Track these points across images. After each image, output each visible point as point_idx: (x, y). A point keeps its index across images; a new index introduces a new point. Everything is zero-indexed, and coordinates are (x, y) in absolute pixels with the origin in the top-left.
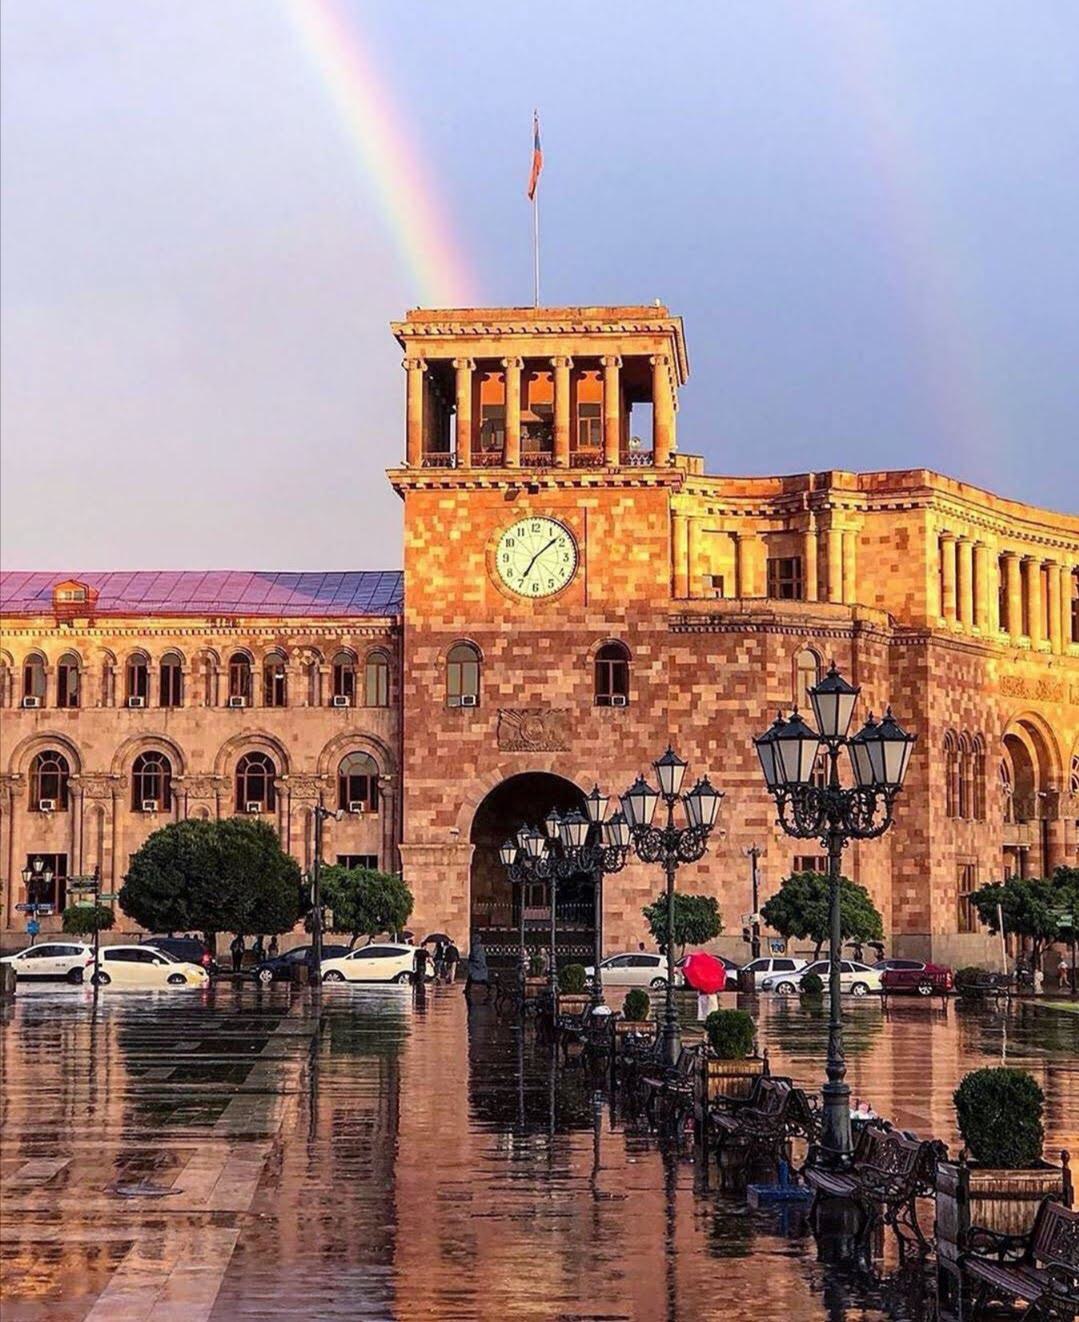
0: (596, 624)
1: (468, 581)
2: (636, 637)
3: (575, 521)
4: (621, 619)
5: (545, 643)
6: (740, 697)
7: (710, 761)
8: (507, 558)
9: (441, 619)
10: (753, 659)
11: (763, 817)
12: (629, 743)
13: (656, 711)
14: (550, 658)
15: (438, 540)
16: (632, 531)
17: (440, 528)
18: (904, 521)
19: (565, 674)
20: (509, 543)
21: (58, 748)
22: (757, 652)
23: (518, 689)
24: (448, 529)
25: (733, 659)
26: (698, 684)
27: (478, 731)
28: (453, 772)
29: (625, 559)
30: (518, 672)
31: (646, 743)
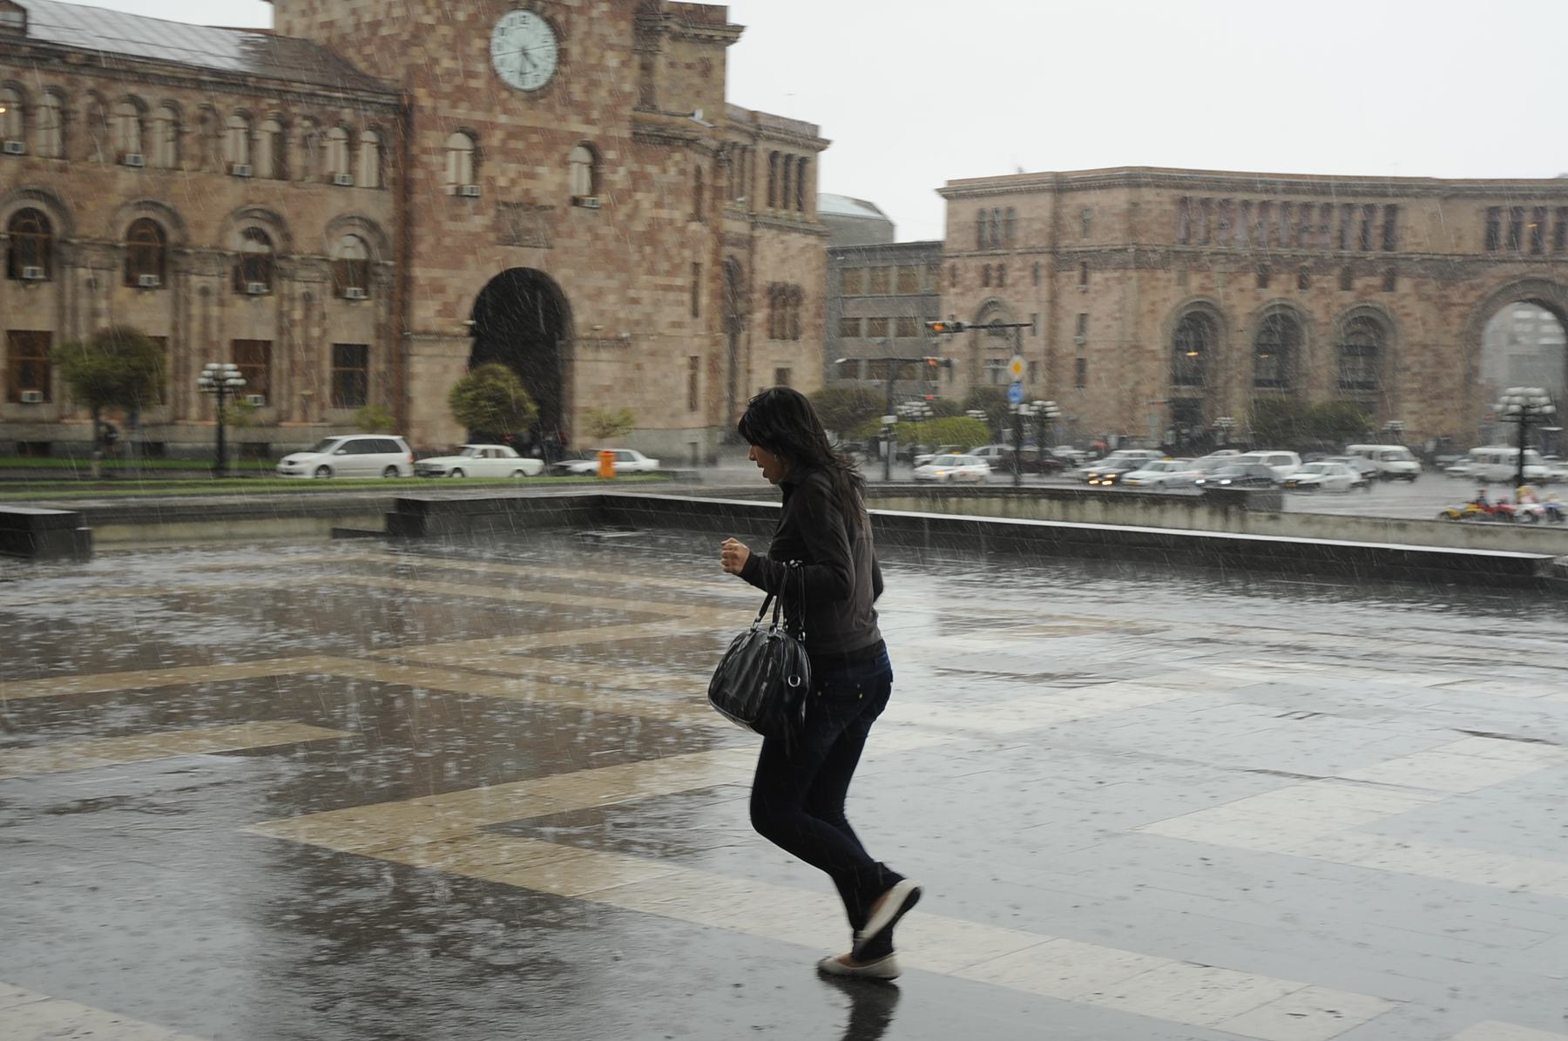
0: (576, 125)
2: (607, 141)
3: (560, 18)
5: (535, 138)
6: (672, 207)
7: (645, 265)
8: (500, 46)
10: (683, 172)
12: (599, 245)
13: (621, 214)
14: (538, 154)
15: (447, 19)
18: (707, 52)
21: (41, 206)
22: (682, 166)
23: (513, 182)
25: (665, 171)
27: (478, 223)
28: (457, 264)
30: (513, 166)
31: (612, 246)
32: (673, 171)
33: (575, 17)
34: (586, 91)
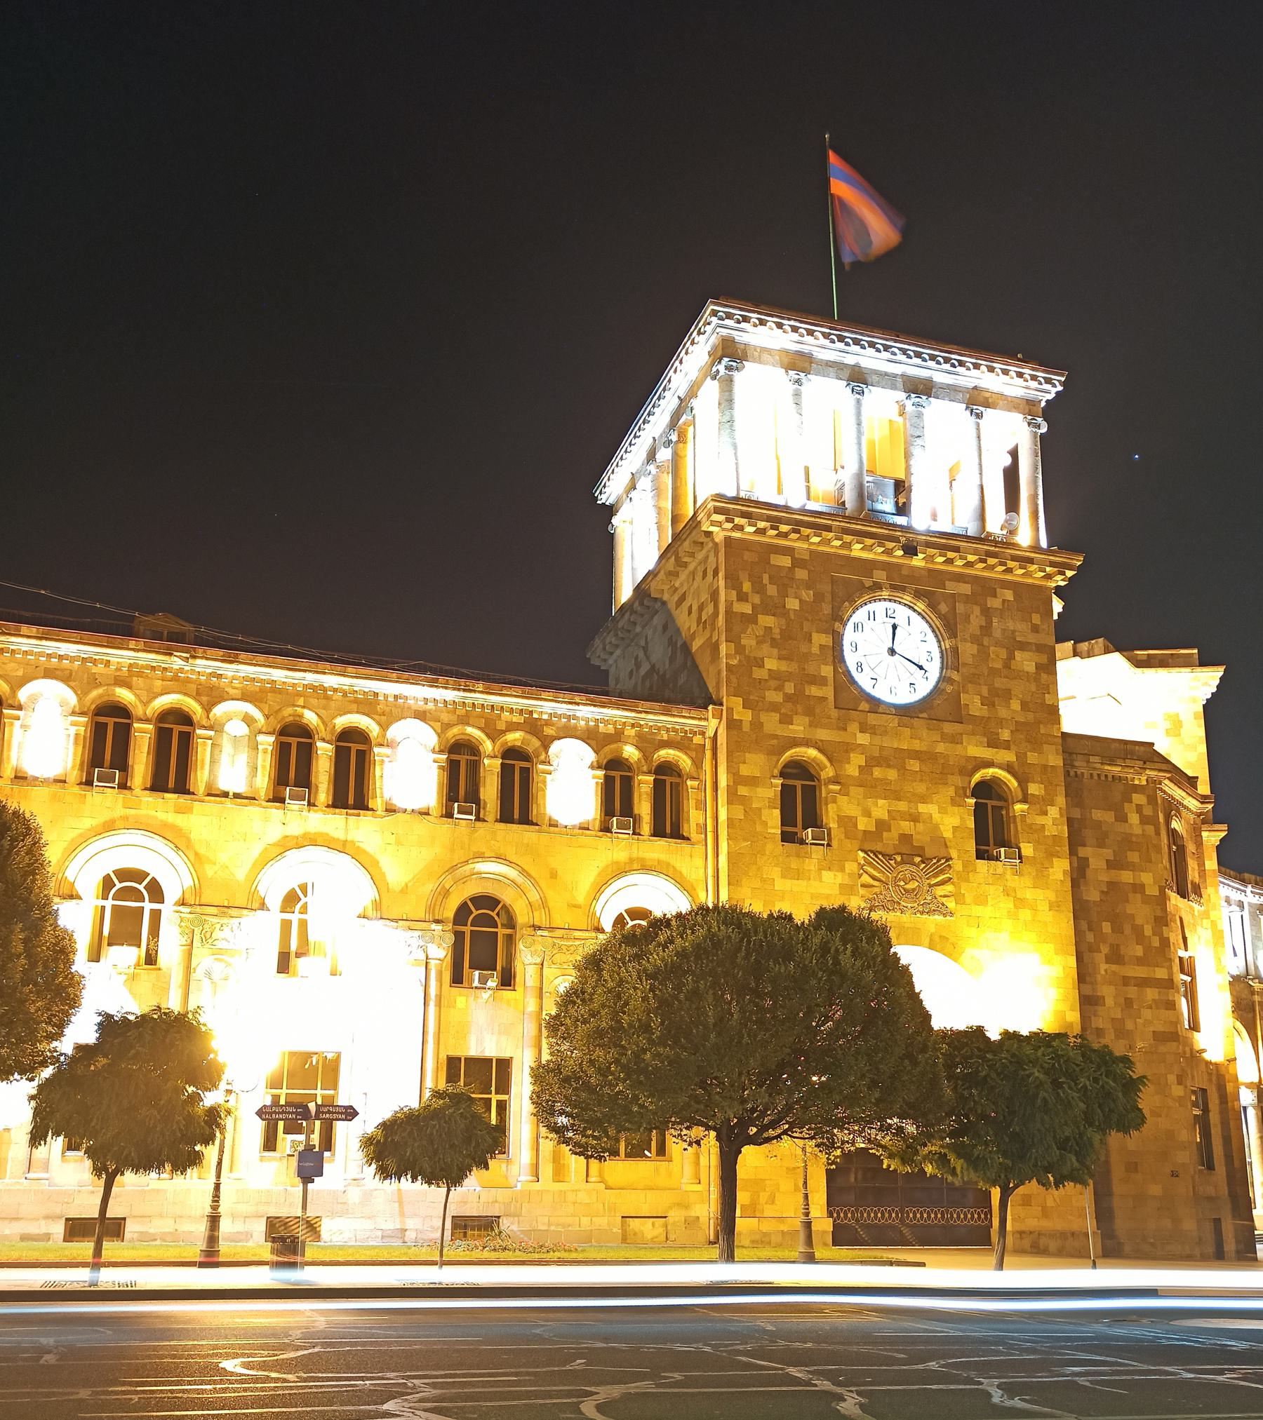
0: (976, 750)
1: (811, 669)
4: (1006, 746)
5: (914, 765)
7: (1105, 949)
9: (776, 716)
10: (1144, 820)
11: (1172, 1030)
14: (921, 788)
16: (1014, 632)
17: (772, 590)
19: (942, 811)
20: (856, 627)
22: (1148, 811)
23: (882, 826)
24: (783, 595)
25: (1122, 818)
26: (1084, 845)
29: (1007, 665)
30: (881, 802)
32: (1134, 818)
33: (960, 608)
34: (987, 702)
